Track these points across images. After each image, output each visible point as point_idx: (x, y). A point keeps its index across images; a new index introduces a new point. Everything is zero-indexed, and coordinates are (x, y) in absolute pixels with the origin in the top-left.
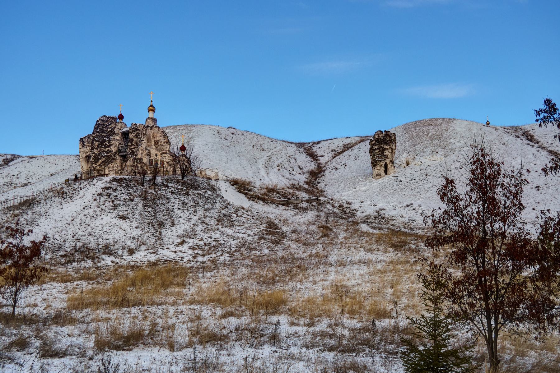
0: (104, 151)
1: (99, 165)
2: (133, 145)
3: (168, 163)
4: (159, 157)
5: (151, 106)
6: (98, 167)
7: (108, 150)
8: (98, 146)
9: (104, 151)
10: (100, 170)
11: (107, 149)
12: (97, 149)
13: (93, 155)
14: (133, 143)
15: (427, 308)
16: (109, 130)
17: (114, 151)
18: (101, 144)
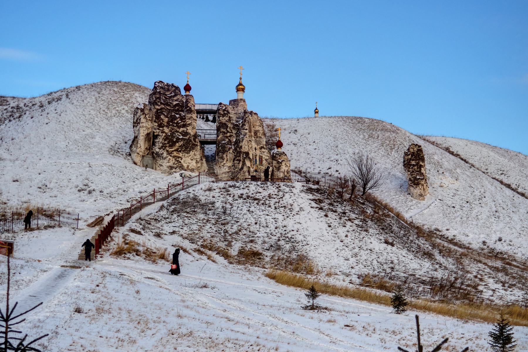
0: (178, 132)
1: (176, 150)
2: (228, 132)
3: (266, 160)
4: (258, 152)
5: (240, 84)
6: (175, 154)
7: (183, 131)
8: (168, 123)
9: (178, 132)
10: (179, 157)
11: (181, 129)
12: (167, 127)
13: (164, 134)
14: (228, 130)
15: (186, 304)
16: (175, 103)
17: (192, 134)
18: (172, 121)
